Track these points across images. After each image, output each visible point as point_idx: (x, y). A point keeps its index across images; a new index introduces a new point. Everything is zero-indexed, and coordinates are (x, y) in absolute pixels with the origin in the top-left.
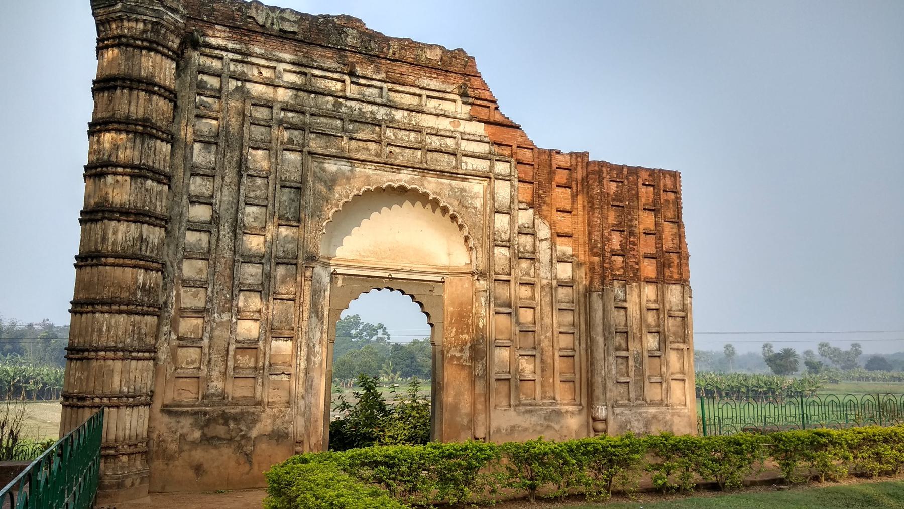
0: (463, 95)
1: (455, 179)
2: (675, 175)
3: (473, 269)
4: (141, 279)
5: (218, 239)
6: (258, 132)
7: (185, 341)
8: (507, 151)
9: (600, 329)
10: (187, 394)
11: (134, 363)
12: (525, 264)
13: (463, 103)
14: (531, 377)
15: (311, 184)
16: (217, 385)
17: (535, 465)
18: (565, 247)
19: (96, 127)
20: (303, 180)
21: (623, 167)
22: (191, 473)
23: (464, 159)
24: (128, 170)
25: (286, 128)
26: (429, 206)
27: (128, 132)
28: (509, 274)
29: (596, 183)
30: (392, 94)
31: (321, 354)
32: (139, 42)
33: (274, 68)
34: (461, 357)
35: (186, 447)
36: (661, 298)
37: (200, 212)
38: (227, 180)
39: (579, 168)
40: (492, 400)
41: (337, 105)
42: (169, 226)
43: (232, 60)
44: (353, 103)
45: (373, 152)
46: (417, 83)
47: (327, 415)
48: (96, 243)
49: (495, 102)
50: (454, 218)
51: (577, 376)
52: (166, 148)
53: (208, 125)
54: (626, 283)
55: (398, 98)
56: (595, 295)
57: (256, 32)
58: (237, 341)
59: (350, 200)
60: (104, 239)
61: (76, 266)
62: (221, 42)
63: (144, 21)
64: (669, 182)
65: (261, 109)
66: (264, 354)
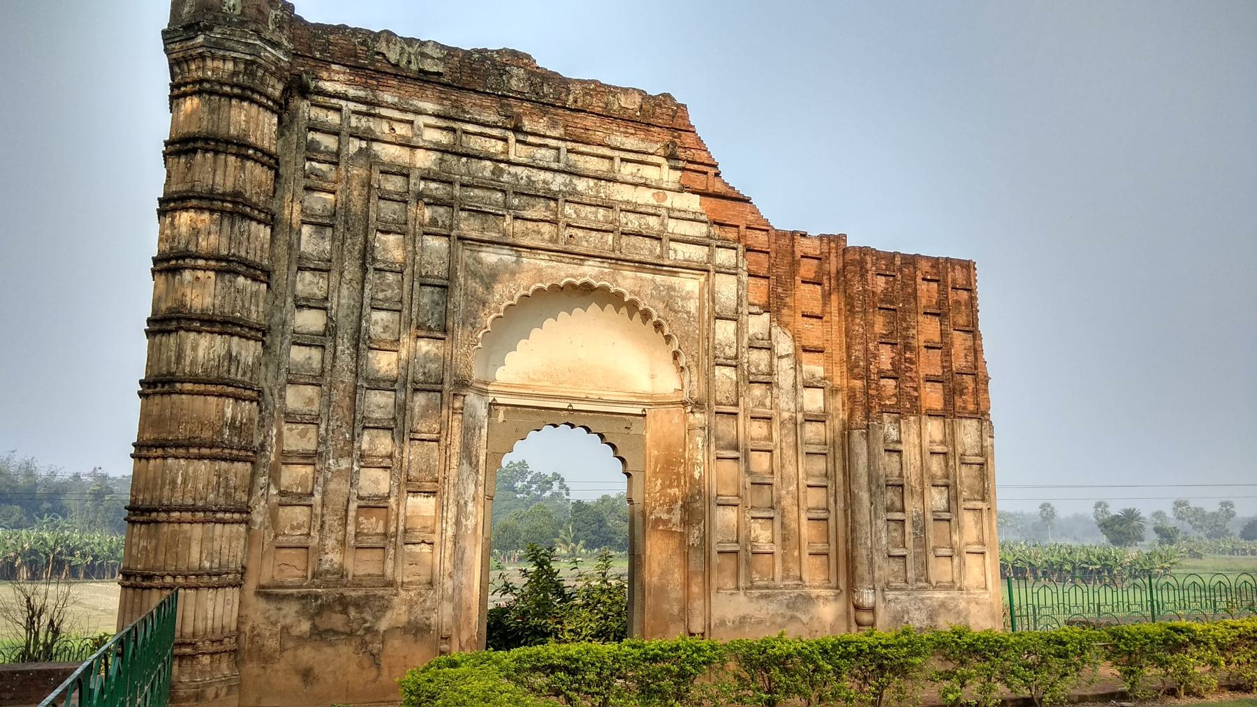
0: (671, 157)
1: (659, 272)
2: (968, 266)
3: (685, 397)
4: (229, 413)
5: (335, 357)
6: (389, 210)
7: (289, 498)
8: (731, 234)
9: (864, 480)
10: (291, 571)
11: (219, 527)
12: (758, 391)
13: (672, 168)
14: (767, 548)
15: (462, 280)
16: (333, 558)
17: (775, 672)
18: (814, 367)
19: (169, 205)
20: (451, 275)
21: (894, 255)
22: (296, 681)
23: (672, 244)
24: (213, 263)
25: (427, 204)
26: (624, 310)
27: (212, 211)
28: (737, 405)
29: (857, 278)
30: (573, 157)
31: (475, 516)
32: (227, 89)
33: (411, 123)
34: (669, 520)
35: (290, 644)
36: (950, 438)
37: (311, 320)
38: (347, 276)
39: (833, 256)
40: (713, 580)
41: (497, 172)
42: (267, 339)
43: (354, 112)
44: (519, 170)
45: (546, 237)
46: (607, 141)
47: (483, 601)
48: (169, 363)
49: (715, 166)
50: (658, 326)
51: (833, 547)
52: (264, 232)
53: (321, 201)
54: (900, 415)
55: (583, 163)
56: (856, 433)
57: (386, 73)
58: (359, 497)
59: (515, 302)
60: (179, 358)
61: (141, 394)
62: (340, 88)
63: (234, 59)
64: (959, 275)
65: (394, 178)
66: (398, 515)
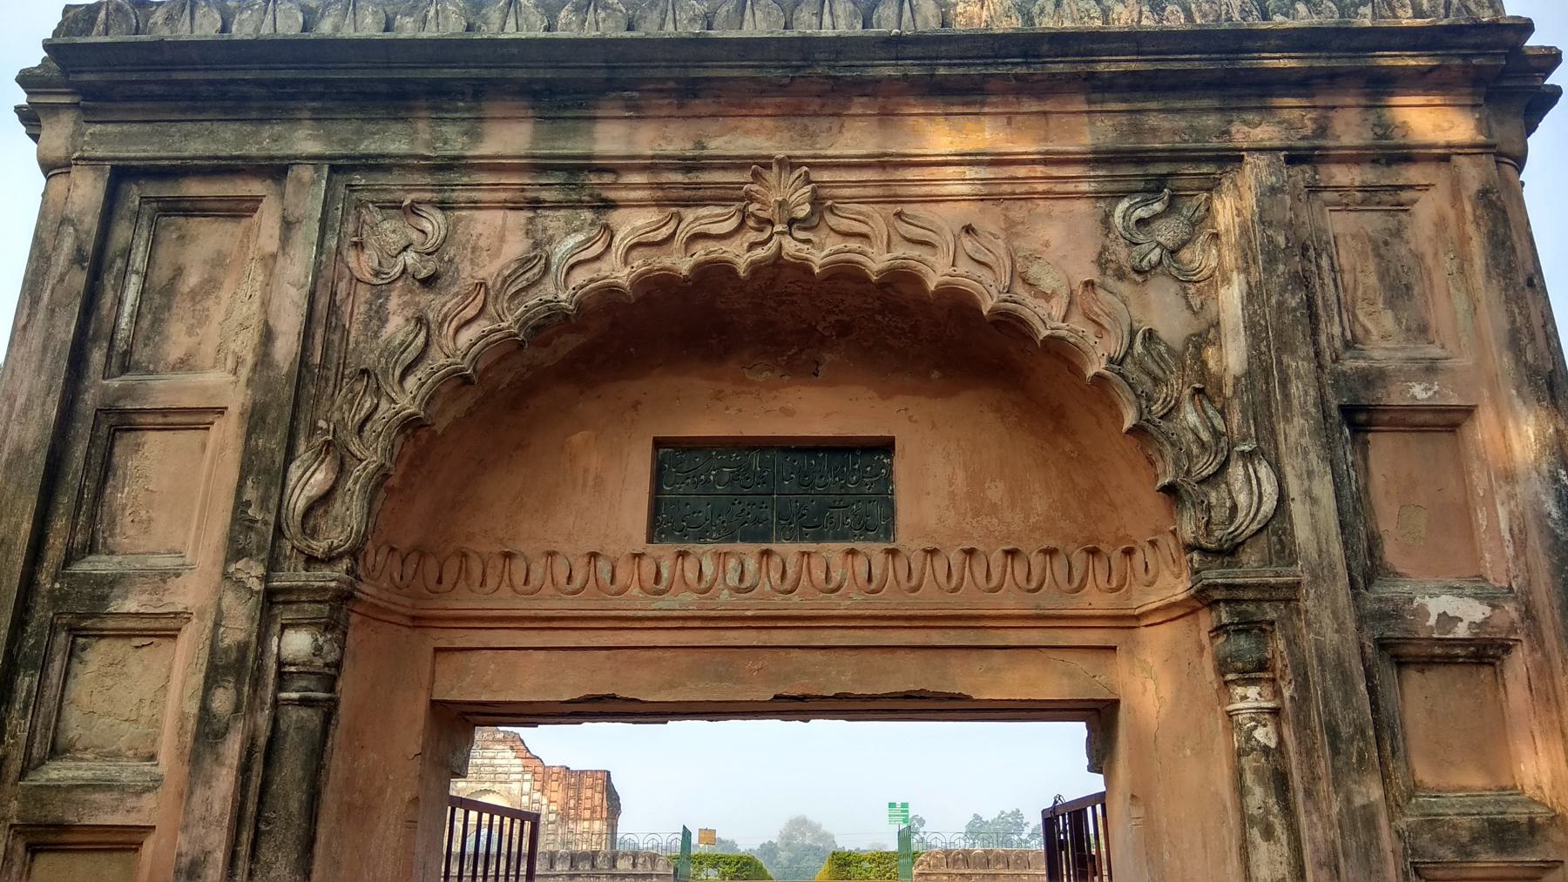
0: (512, 748)
18: (553, 807)
